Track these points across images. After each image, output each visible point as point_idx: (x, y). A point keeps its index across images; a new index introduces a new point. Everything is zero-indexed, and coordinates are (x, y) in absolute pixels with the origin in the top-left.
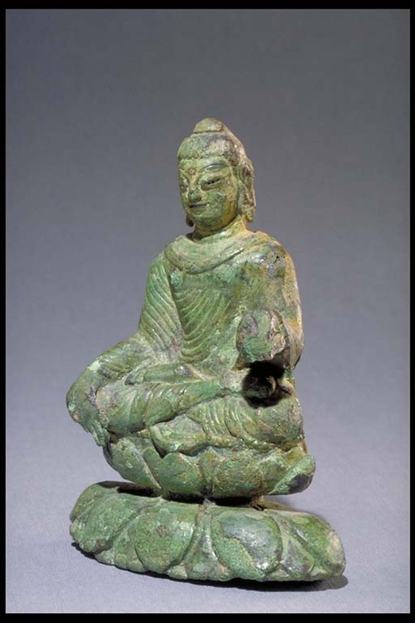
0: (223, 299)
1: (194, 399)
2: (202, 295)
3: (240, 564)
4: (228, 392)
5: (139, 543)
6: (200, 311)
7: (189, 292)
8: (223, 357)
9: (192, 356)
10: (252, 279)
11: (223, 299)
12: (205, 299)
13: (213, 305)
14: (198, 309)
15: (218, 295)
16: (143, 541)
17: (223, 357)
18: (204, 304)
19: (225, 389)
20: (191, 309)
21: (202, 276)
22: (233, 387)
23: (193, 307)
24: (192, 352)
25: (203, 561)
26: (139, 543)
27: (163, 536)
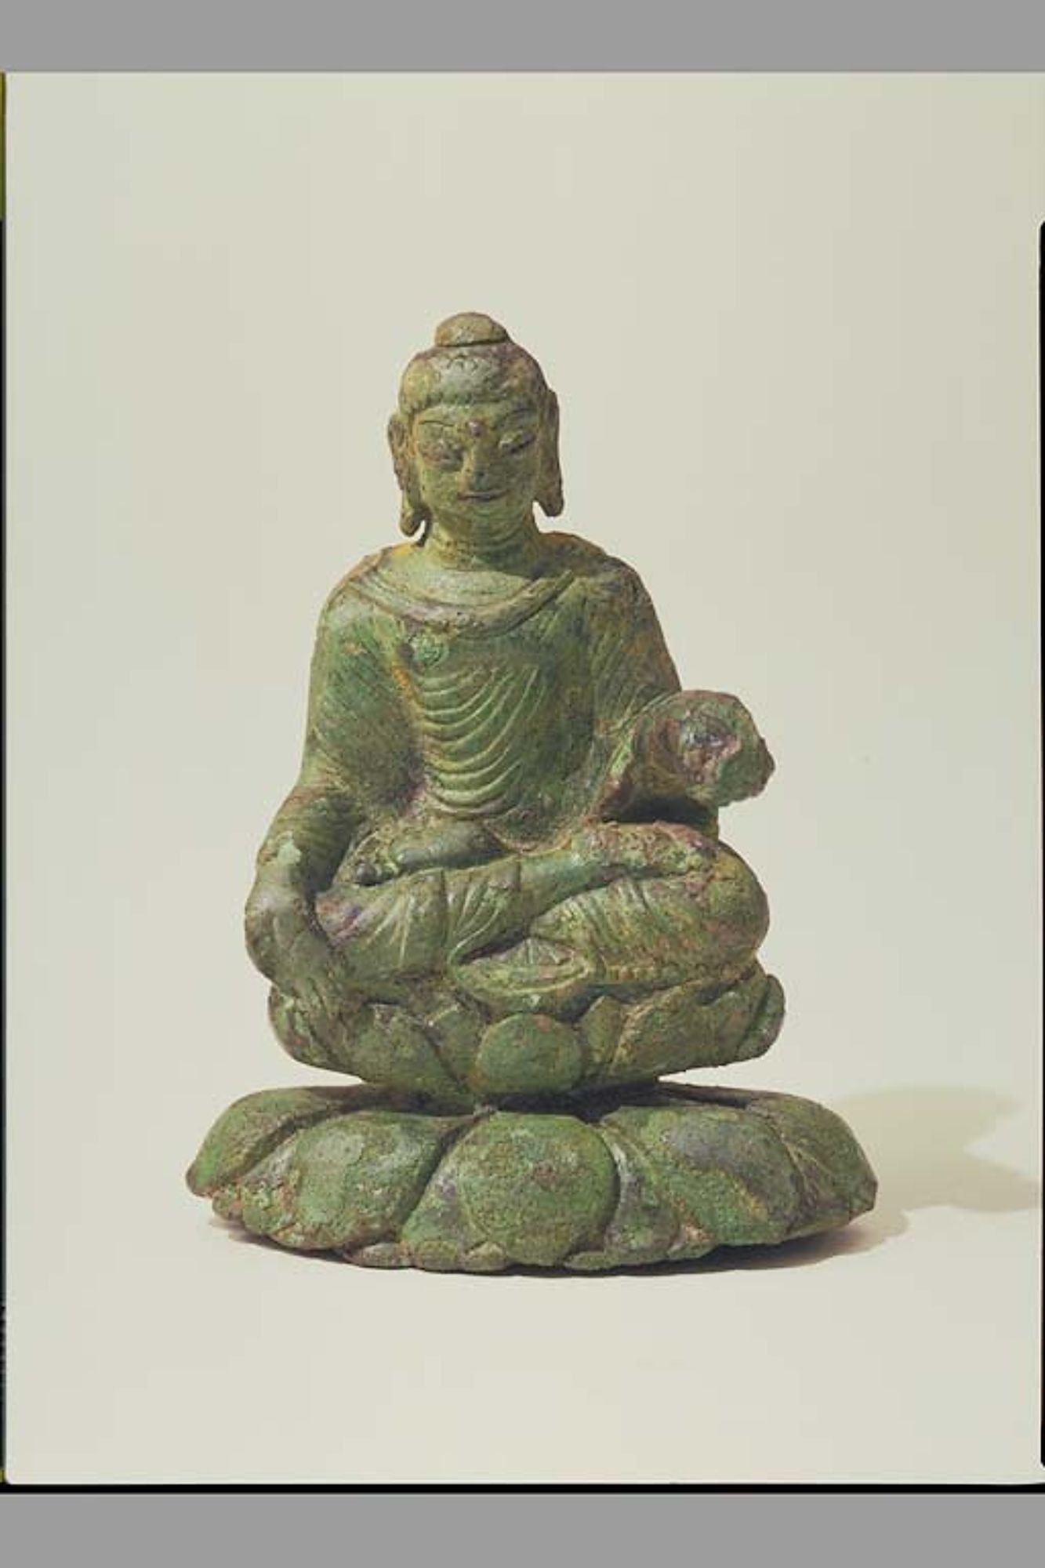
0: (544, 680)
1: (543, 895)
2: (498, 679)
3: (736, 1218)
4: (620, 871)
5: (491, 1211)
6: (495, 712)
7: (466, 675)
8: (548, 800)
9: (477, 806)
10: (598, 633)
11: (544, 680)
12: (506, 684)
13: (525, 695)
14: (490, 708)
15: (534, 675)
16: (501, 1207)
17: (548, 800)
18: (505, 697)
19: (613, 865)
20: (472, 709)
21: (498, 639)
22: (629, 860)
23: (478, 703)
24: (479, 797)
25: (650, 1226)
26: (491, 1211)
27: (553, 1187)
